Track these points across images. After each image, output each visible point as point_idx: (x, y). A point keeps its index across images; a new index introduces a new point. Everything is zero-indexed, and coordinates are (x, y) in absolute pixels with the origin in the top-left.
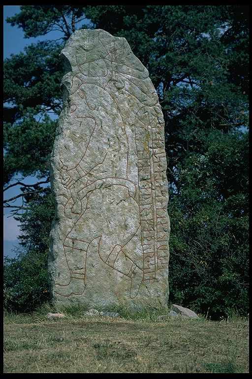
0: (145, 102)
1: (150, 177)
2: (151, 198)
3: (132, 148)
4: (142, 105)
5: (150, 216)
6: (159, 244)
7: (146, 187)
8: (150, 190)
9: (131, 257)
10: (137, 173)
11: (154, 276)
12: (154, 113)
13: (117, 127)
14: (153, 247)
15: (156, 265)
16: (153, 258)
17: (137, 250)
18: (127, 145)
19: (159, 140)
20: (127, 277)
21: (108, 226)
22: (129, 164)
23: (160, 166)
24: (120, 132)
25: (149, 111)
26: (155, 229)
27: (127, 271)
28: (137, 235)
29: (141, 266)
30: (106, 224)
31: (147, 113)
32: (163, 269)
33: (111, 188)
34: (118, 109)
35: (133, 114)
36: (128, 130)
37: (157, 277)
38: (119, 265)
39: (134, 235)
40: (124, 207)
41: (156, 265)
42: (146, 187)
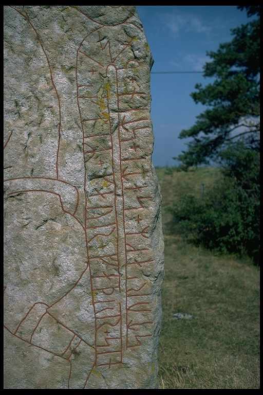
0: (101, 18)
1: (110, 171)
2: (113, 214)
3: (70, 114)
4: (92, 25)
5: (110, 249)
6: (131, 302)
7: (102, 192)
8: (111, 198)
9: (69, 325)
10: (79, 166)
11: (118, 358)
12: (123, 37)
13: (35, 77)
14: (117, 306)
15: (124, 340)
16: (117, 327)
17: (83, 311)
18: (57, 110)
19: (134, 92)
20: (60, 360)
21: (18, 269)
22: (62, 149)
23: (135, 146)
24: (42, 85)
25: (110, 35)
26: (123, 272)
27: (61, 350)
28: (81, 285)
29: (91, 341)
30: (14, 265)
31: (105, 41)
32: (140, 346)
33: (22, 197)
34: (38, 38)
35: (72, 46)
36: (61, 80)
37: (125, 360)
38: (44, 337)
39: (75, 284)
40: (52, 233)
41: (124, 340)
42: (102, 192)
